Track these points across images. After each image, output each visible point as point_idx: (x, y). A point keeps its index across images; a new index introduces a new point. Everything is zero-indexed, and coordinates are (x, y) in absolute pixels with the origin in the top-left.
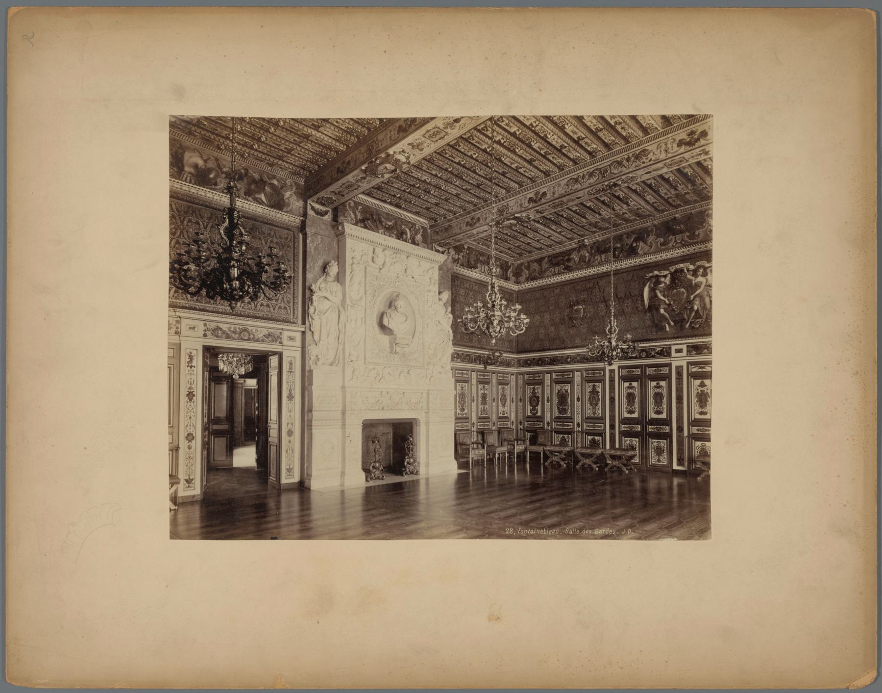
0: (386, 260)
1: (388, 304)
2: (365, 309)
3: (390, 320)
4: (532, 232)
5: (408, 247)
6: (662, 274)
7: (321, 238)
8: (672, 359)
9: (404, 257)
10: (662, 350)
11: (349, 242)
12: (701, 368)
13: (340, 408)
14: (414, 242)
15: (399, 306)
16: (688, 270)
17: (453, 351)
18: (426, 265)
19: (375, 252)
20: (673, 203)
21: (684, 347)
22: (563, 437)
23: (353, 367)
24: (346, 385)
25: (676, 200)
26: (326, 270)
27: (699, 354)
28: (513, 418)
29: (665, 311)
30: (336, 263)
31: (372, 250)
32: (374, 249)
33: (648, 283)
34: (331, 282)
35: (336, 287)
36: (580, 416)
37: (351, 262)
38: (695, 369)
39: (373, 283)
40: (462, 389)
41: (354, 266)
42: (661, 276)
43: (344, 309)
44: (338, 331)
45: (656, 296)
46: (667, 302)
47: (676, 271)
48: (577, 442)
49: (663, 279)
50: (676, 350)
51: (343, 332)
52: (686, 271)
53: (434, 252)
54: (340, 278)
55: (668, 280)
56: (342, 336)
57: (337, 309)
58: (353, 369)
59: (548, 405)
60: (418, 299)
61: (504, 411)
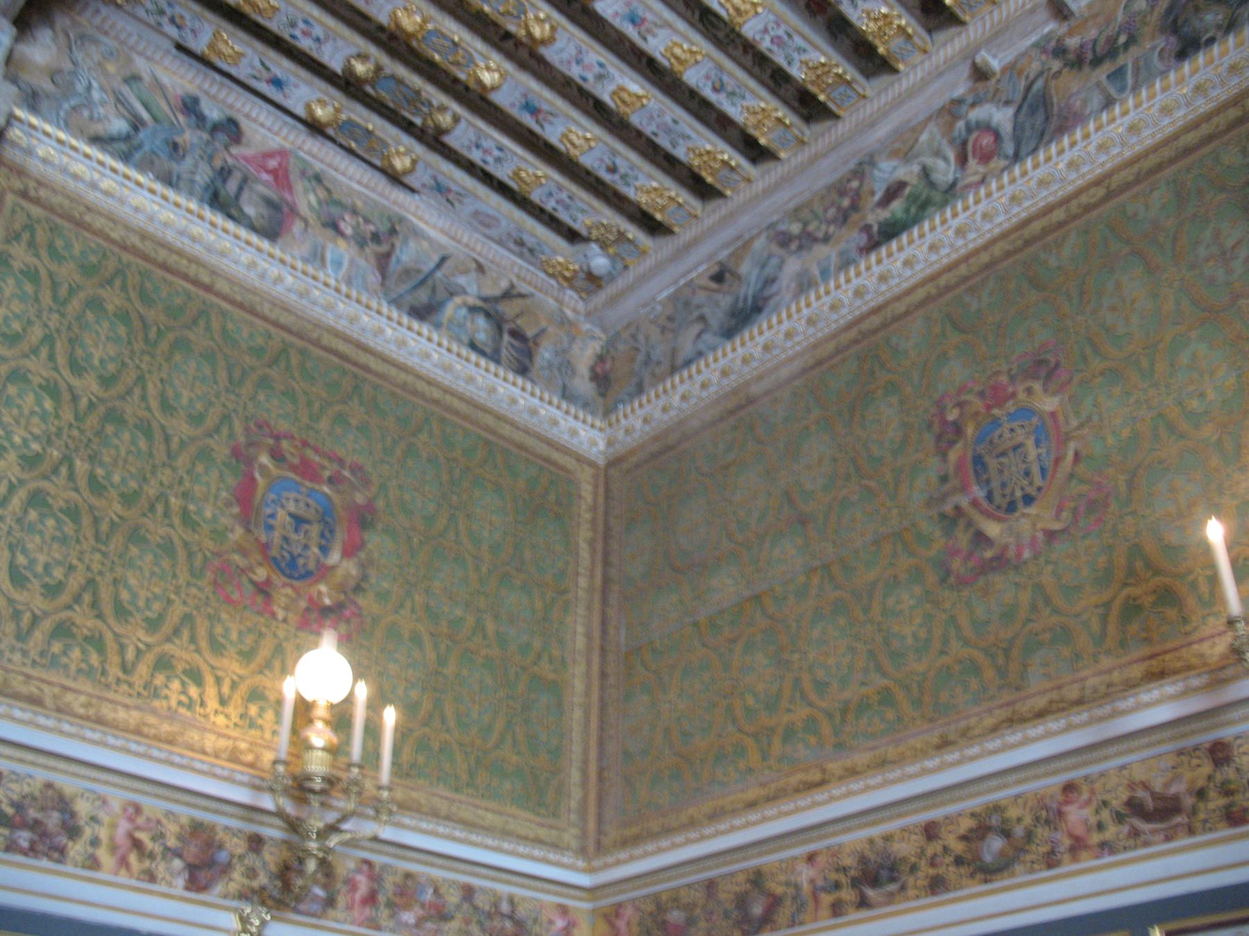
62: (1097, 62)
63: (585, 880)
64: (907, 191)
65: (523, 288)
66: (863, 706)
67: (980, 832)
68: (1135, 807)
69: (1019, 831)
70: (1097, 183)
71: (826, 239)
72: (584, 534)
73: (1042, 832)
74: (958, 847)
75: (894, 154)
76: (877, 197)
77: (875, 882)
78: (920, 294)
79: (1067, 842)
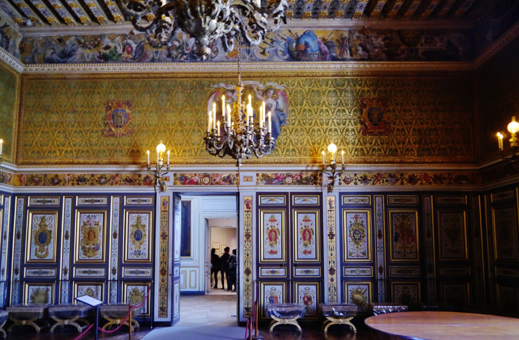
6: (230, 88)
10: (229, 177)
12: (271, 200)
16: (258, 90)
21: (254, 174)
27: (269, 184)
33: (213, 96)
38: (264, 201)
50: (244, 177)
52: (255, 89)
62: (154, 47)
63: (16, 169)
64: (111, 49)
65: (8, 24)
66: (83, 151)
67: (101, 177)
68: (126, 180)
69: (108, 179)
70: (147, 74)
71: (90, 49)
72: (17, 91)
73: (111, 180)
74: (97, 179)
75: (109, 38)
76: (104, 46)
77: (81, 181)
78: (109, 76)
79: (115, 182)
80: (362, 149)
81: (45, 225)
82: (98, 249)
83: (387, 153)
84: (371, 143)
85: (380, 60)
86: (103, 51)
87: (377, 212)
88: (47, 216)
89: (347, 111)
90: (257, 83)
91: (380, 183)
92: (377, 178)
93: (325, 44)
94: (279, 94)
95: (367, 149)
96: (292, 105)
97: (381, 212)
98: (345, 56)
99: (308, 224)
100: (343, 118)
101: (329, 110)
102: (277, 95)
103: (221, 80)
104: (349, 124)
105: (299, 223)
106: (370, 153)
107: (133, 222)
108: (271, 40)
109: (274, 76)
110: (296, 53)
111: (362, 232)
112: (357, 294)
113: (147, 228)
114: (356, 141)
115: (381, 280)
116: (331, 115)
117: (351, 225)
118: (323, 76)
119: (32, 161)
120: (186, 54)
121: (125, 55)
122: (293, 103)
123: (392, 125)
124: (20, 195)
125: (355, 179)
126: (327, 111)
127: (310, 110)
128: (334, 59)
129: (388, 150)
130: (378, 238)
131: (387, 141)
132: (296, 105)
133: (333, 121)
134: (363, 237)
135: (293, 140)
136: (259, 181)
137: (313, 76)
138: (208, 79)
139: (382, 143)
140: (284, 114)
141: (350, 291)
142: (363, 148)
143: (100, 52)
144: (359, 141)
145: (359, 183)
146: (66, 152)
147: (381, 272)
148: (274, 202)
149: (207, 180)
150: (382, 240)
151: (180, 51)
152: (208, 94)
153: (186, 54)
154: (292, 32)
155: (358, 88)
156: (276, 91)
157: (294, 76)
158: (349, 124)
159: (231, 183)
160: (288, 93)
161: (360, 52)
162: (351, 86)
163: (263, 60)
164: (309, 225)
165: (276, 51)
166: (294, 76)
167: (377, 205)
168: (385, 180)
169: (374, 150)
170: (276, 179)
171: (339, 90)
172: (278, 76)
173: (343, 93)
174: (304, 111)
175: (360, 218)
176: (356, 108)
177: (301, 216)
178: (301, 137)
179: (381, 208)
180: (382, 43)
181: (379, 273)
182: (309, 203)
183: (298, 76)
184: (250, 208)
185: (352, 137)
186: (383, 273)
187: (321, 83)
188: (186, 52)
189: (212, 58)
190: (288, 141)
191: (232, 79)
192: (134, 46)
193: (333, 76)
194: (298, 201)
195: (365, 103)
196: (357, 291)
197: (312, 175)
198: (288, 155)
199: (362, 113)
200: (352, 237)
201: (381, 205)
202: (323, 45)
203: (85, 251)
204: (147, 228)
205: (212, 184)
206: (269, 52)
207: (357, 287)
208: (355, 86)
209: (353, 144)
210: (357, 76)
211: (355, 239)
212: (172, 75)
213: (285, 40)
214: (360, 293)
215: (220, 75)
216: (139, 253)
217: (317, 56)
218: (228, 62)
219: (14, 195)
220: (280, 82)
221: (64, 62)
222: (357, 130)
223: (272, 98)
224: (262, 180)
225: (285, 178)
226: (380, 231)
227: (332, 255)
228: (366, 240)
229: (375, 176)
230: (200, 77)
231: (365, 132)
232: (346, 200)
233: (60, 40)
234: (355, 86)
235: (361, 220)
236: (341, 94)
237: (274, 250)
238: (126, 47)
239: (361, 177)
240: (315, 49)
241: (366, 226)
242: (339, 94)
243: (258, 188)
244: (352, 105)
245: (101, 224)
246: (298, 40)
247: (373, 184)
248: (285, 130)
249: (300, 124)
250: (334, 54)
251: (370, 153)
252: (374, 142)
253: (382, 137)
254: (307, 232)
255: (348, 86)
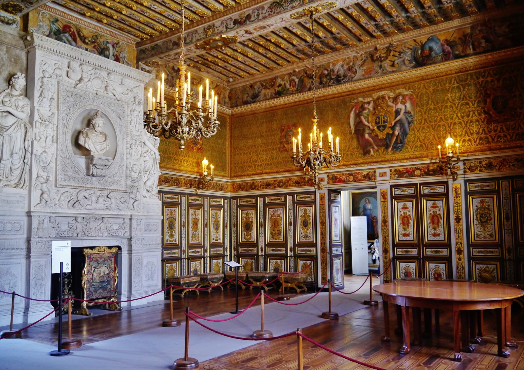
0: (84, 76)
1: (86, 122)
2: (57, 126)
3: (87, 138)
4: (242, 56)
5: (110, 63)
6: (366, 101)
7: (7, 48)
8: (377, 183)
9: (104, 74)
10: (368, 174)
11: (39, 55)
12: (403, 191)
13: (25, 236)
14: (117, 59)
15: (97, 125)
16: (389, 98)
17: (160, 174)
18: (129, 83)
19: (71, 66)
20: (374, 34)
21: (387, 171)
22: (276, 262)
23: (41, 190)
24: (32, 210)
25: (376, 31)
26: (11, 83)
27: (401, 177)
28: (227, 245)
29: (369, 136)
30: (24, 75)
31: (67, 64)
32: (69, 62)
33: (354, 109)
34: (17, 96)
35: (23, 101)
36: (292, 240)
37: (42, 75)
38: (398, 192)
39: (68, 99)
40: (171, 215)
41: (45, 80)
42: (365, 103)
43: (32, 124)
44: (24, 150)
45: (361, 122)
46: (371, 127)
47: (378, 98)
48: (290, 267)
49: (366, 106)
50: (380, 173)
51: (30, 151)
52: (387, 98)
53: (140, 71)
54: (28, 92)
55: (371, 107)
56: (28, 155)
57: (23, 125)
58: (41, 192)
59: (261, 230)
60: (119, 117)
61: (217, 237)
63: (230, 181)
66: (268, 164)
67: (280, 182)
68: (296, 182)
70: (306, 100)
71: (269, 89)
72: (228, 128)
75: (281, 78)
78: (281, 107)
80: (487, 138)
81: (249, 218)
82: (280, 234)
83: (513, 138)
84: (495, 131)
85: (505, 48)
86: (277, 89)
87: (504, 196)
88: (250, 211)
89: (471, 104)
90: (388, 92)
91: (506, 168)
92: (502, 163)
93: (447, 45)
94: (407, 98)
95: (492, 137)
96: (419, 106)
97: (508, 196)
98: (468, 52)
99: (437, 210)
100: (467, 110)
101: (453, 105)
102: (406, 100)
103: (359, 95)
104: (473, 116)
105: (428, 210)
106: (495, 141)
107: (302, 214)
108: (399, 52)
109: (403, 84)
110: (421, 59)
111: (488, 215)
112: (485, 272)
113: (311, 217)
114: (481, 131)
115: (510, 260)
116: (455, 109)
117: (477, 209)
118: (446, 75)
119: (239, 174)
120: (332, 79)
121: (292, 88)
122: (420, 104)
123: (518, 109)
124: (234, 198)
125: (480, 167)
126: (451, 106)
127: (435, 109)
128: (457, 57)
129: (514, 135)
130: (505, 220)
131: (514, 126)
132: (423, 106)
133: (457, 115)
134: (490, 220)
135: (420, 137)
136: (393, 176)
137: (437, 77)
138: (349, 96)
139: (508, 129)
140: (411, 116)
141: (478, 269)
142: (488, 136)
143: (275, 90)
144: (483, 130)
145: (484, 169)
146: (258, 165)
147: (509, 253)
148: (406, 193)
149: (351, 178)
150: (510, 222)
151: (328, 77)
152: (350, 109)
153: (332, 79)
154: (417, 41)
155: (481, 79)
156: (404, 97)
157: (420, 80)
158: (473, 116)
159: (370, 179)
160: (415, 96)
161: (483, 45)
162: (474, 79)
163: (393, 72)
164: (437, 211)
165: (404, 61)
166: (420, 80)
167: (503, 189)
168: (511, 164)
169: (499, 137)
170: (406, 172)
171: (462, 85)
172: (405, 83)
173: (467, 88)
174: (429, 111)
175: (487, 202)
176: (480, 99)
177: (430, 203)
178: (428, 134)
179: (508, 192)
180: (507, 30)
181: (507, 255)
182: (436, 191)
183: (423, 80)
184: (386, 199)
185: (477, 127)
186: (512, 254)
187: (444, 81)
188: (333, 77)
189: (352, 78)
190: (416, 139)
191: (367, 93)
192: (297, 80)
193: (456, 73)
194: (427, 190)
195: (489, 93)
196: (485, 270)
197: (438, 166)
198: (417, 151)
199: (485, 103)
200: (478, 221)
201: (508, 189)
202: (446, 46)
203: (273, 235)
204: (311, 217)
205: (355, 181)
206: (397, 63)
207: (484, 266)
208: (478, 78)
209: (478, 133)
210: (480, 68)
211: (482, 222)
212: (323, 98)
213: (411, 49)
214: (488, 272)
215: (359, 91)
216: (306, 236)
217: (440, 57)
218: (365, 79)
219: (230, 198)
220: (407, 88)
221: (254, 102)
222: (481, 120)
223: (401, 103)
224: (394, 175)
225: (414, 171)
226: (507, 214)
227: (459, 237)
228: (493, 223)
229: (500, 162)
230: (344, 96)
231: (489, 120)
232: (472, 187)
233: (251, 86)
234: (478, 78)
235: (487, 204)
236: (464, 88)
237: (407, 232)
238: (292, 82)
239: (486, 164)
240: (438, 52)
241: (492, 210)
242: (462, 89)
243: (391, 181)
244: (476, 97)
245: (282, 216)
246: (423, 46)
247: (499, 169)
248: (413, 130)
249: (427, 122)
250: (457, 52)
251: (495, 141)
252: (499, 129)
253: (508, 123)
254: (435, 217)
255: (471, 80)
